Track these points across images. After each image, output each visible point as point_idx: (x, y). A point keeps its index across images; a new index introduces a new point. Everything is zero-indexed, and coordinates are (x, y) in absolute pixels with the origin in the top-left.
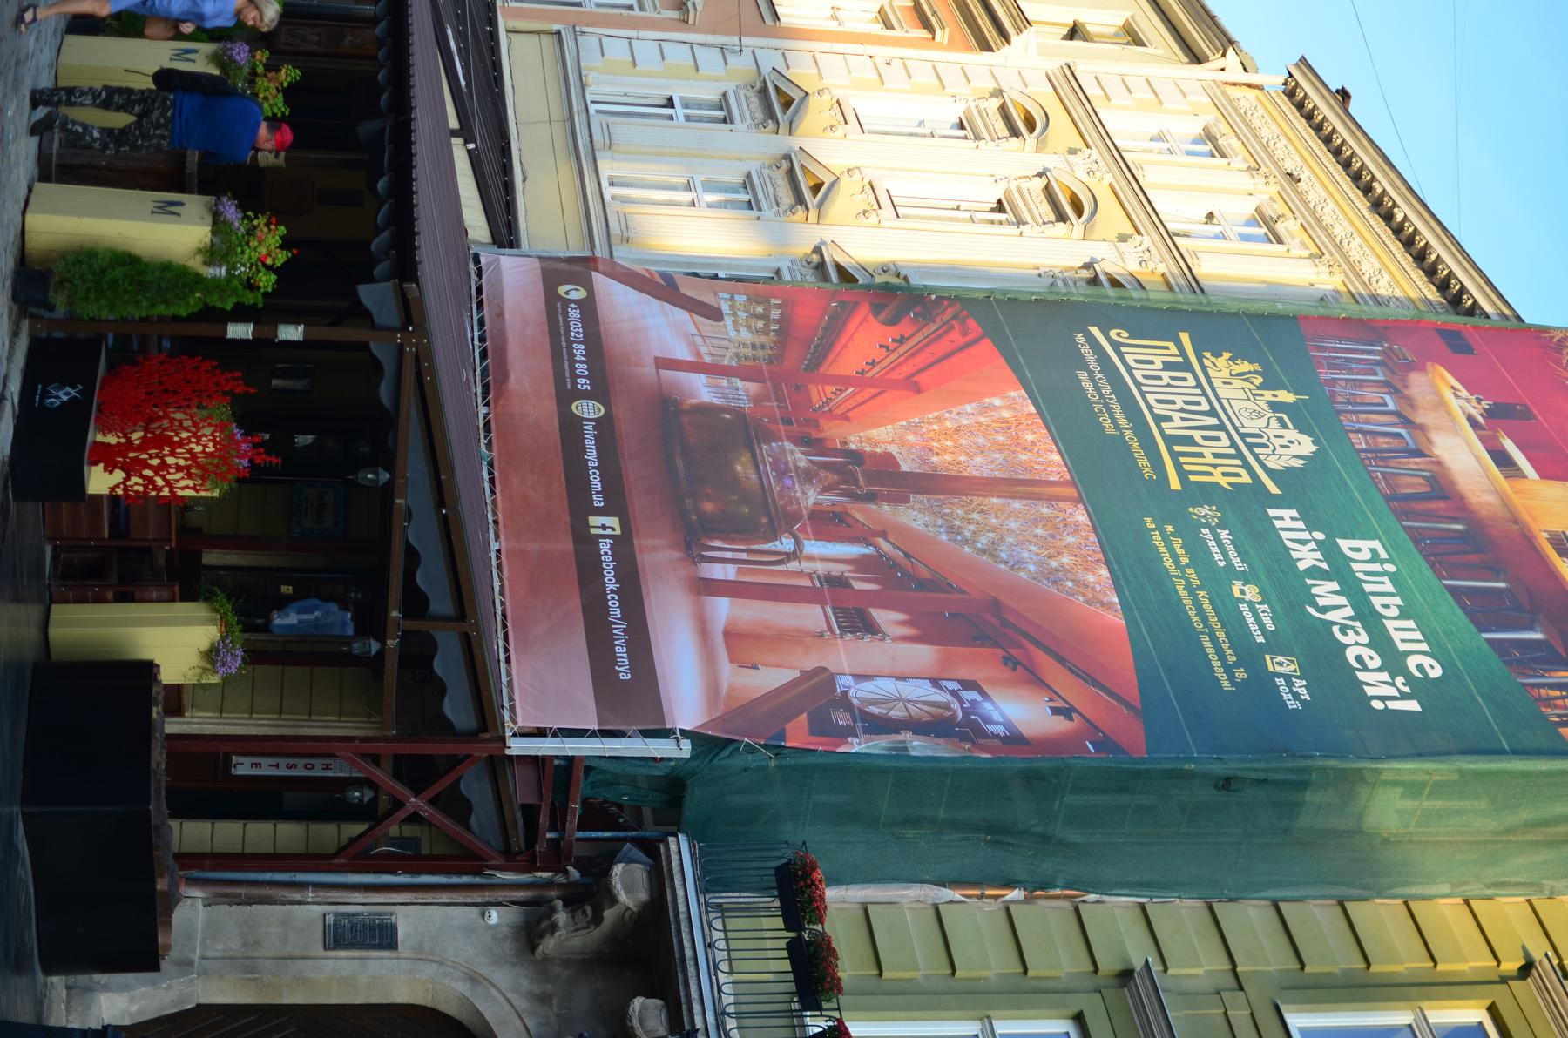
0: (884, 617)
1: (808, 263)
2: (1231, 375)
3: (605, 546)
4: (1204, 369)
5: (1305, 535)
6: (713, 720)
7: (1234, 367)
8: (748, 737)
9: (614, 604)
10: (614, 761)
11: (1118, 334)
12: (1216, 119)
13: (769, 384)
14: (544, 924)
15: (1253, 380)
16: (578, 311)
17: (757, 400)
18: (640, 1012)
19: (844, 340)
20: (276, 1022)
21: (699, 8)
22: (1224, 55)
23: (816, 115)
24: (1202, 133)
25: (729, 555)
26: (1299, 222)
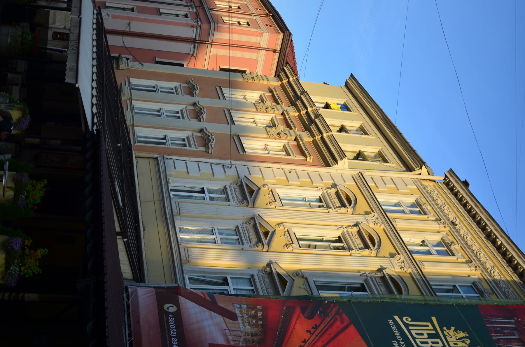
1: (265, 272)
2: (457, 339)
4: (445, 336)
7: (457, 335)
11: (407, 319)
12: (420, 196)
15: (466, 342)
16: (173, 319)
19: (291, 329)
21: (213, 146)
22: (421, 168)
23: (263, 198)
24: (415, 202)
26: (460, 245)
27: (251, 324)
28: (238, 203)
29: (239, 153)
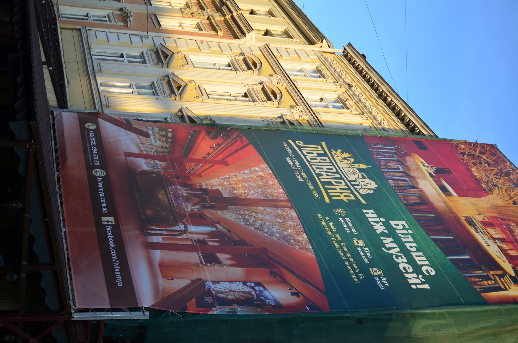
0: (222, 256)
1: (177, 115)
2: (342, 158)
3: (109, 229)
4: (332, 156)
5: (378, 220)
6: (157, 303)
7: (343, 155)
9: (114, 253)
11: (299, 143)
12: (320, 64)
13: (169, 162)
15: (350, 160)
16: (93, 134)
17: (165, 169)
19: (196, 146)
21: (132, 22)
22: (322, 42)
23: (177, 60)
24: (316, 69)
25: (159, 232)
26: (354, 101)
27: (162, 140)
28: (154, 65)
29: (156, 27)
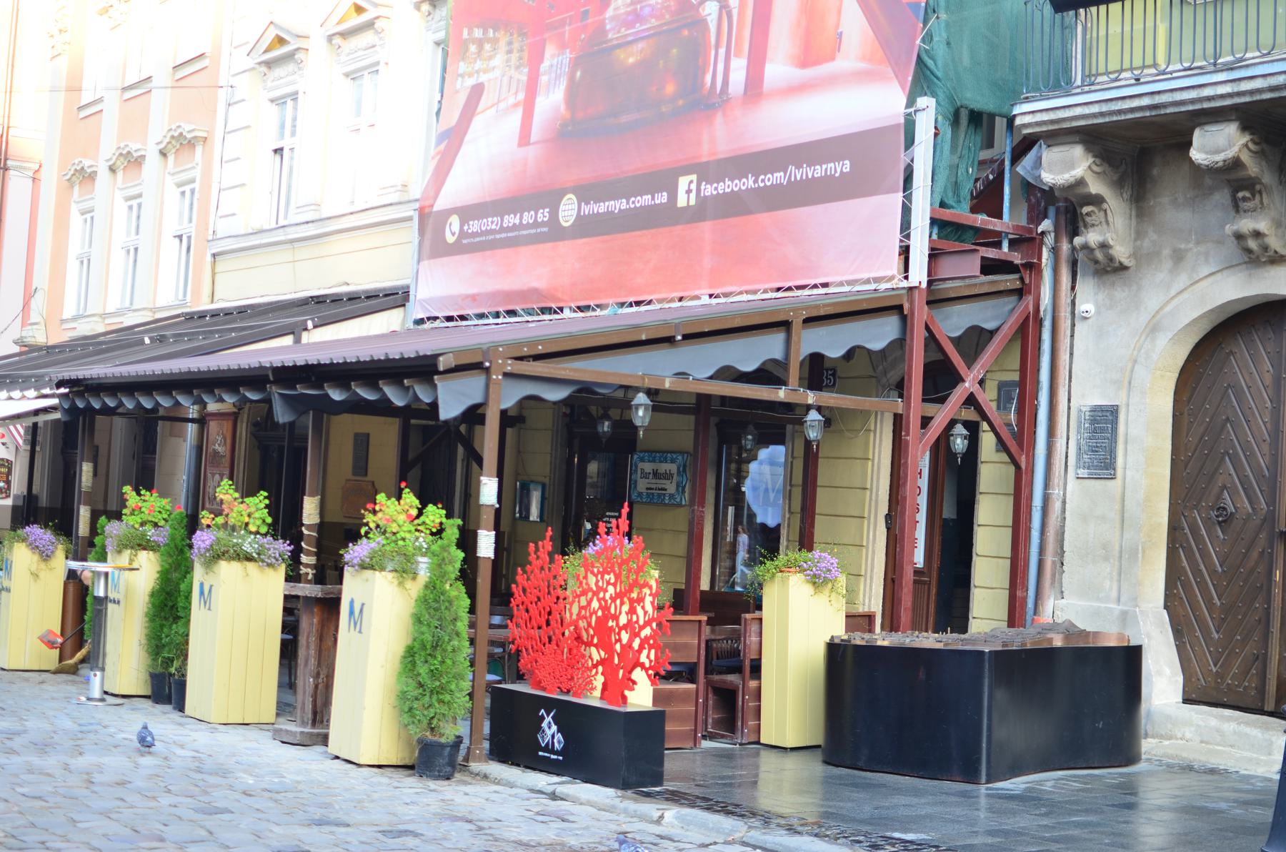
1: (429, 14)
3: (708, 190)
6: (897, 77)
8: (915, 39)
9: (769, 180)
10: (936, 178)
13: (546, 36)
14: (1099, 255)
16: (471, 223)
17: (562, 46)
18: (1207, 153)
20: (1187, 530)
21: (192, 127)
25: (721, 67)
27: (492, 53)
28: (301, 72)
29: (206, 67)
